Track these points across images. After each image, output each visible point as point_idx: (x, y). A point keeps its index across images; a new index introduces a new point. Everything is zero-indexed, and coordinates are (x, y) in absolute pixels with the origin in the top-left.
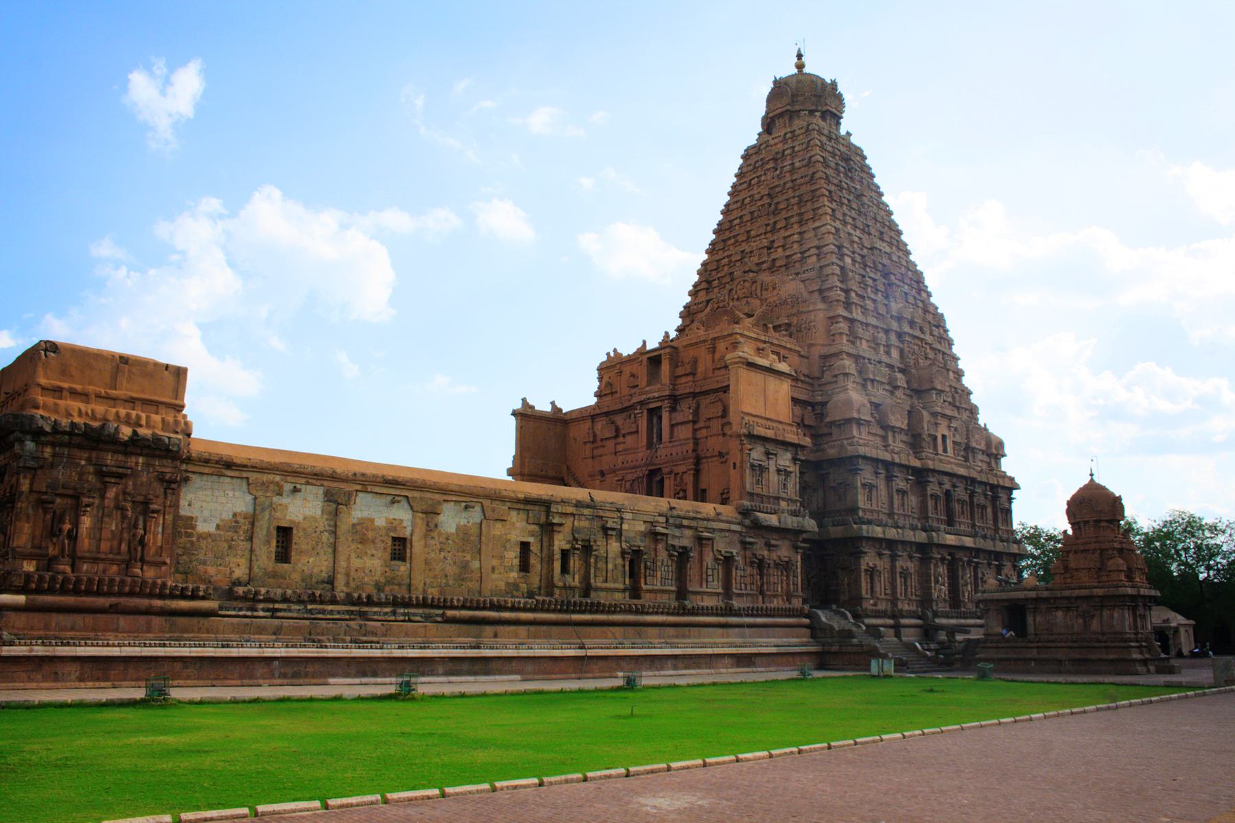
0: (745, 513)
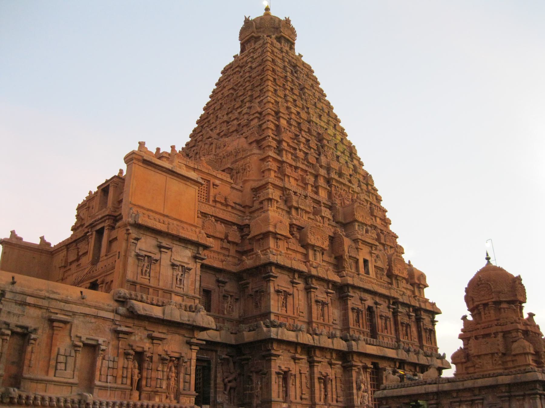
0: (122, 301)
